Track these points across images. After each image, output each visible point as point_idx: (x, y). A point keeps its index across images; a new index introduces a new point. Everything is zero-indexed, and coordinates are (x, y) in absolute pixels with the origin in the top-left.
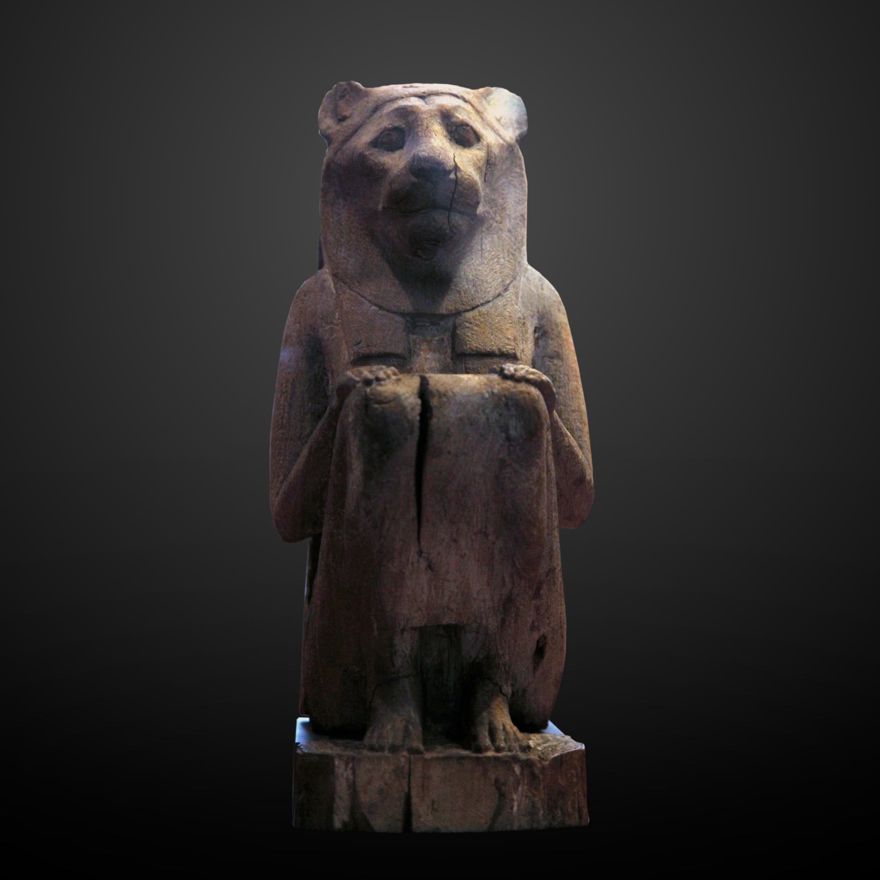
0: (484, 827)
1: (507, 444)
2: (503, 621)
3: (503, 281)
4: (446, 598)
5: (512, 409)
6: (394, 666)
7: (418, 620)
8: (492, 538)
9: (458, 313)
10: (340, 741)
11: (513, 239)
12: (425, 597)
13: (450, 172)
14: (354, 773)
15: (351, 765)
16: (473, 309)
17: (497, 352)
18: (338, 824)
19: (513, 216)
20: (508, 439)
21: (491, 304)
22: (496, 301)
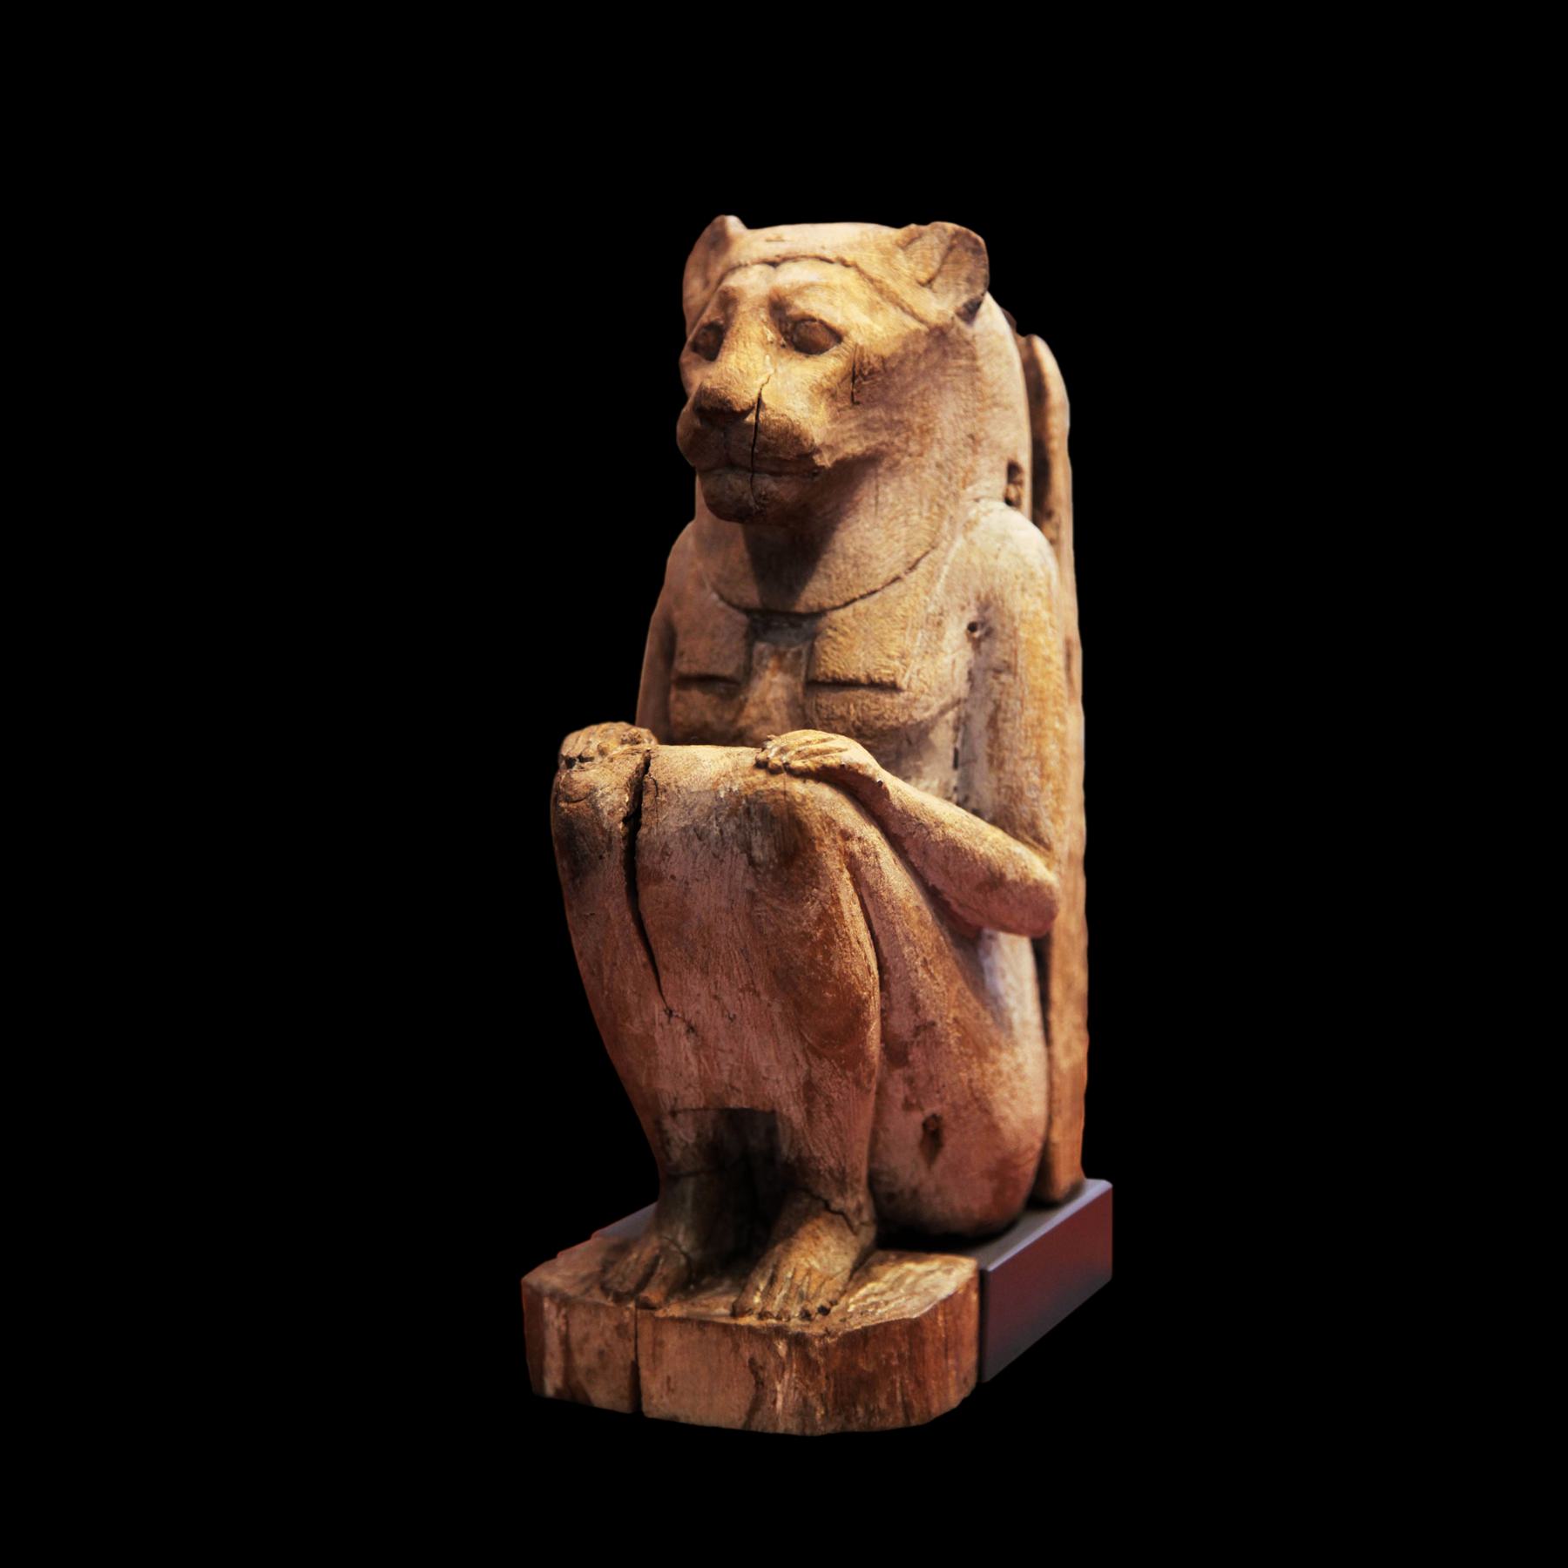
0: (738, 1425)
1: (751, 870)
2: (809, 1113)
3: (908, 555)
4: (726, 1074)
5: (756, 819)
6: (669, 1159)
7: (692, 1098)
8: (765, 998)
9: (821, 612)
11: (945, 480)
12: (694, 1069)
13: (745, 413)
14: (567, 1324)
15: (563, 1311)
16: (847, 604)
17: (863, 679)
18: (550, 1391)
19: (949, 440)
20: (752, 862)
21: (877, 596)
22: (887, 590)
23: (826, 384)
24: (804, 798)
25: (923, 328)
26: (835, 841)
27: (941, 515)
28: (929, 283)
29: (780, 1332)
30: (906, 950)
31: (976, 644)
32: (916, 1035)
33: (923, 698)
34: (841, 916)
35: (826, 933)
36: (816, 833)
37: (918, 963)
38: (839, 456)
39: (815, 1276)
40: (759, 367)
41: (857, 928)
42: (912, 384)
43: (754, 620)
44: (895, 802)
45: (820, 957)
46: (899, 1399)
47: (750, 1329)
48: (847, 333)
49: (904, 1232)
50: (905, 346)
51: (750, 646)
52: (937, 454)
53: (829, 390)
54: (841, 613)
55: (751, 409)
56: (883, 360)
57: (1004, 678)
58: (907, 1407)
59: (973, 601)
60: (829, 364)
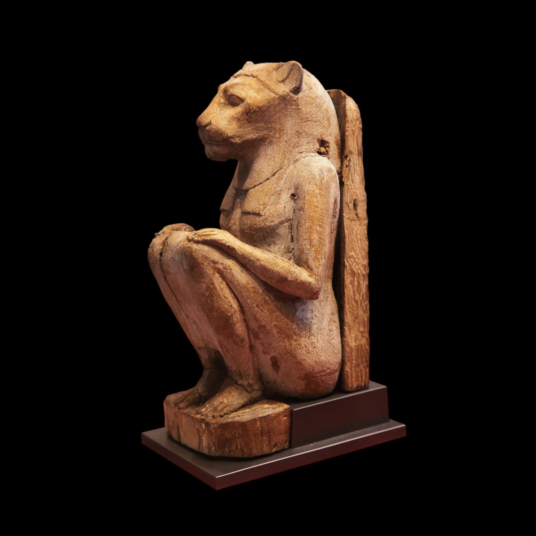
10: (223, 386)
16: (254, 187)
17: (251, 212)
22: (265, 183)
23: (236, 116)
24: (196, 250)
25: (277, 96)
26: (209, 264)
27: (285, 158)
28: (283, 81)
29: (203, 420)
30: (249, 301)
31: (295, 200)
32: (259, 329)
33: (270, 218)
34: (215, 288)
35: (210, 294)
36: (200, 261)
37: (255, 305)
38: (245, 139)
39: (223, 404)
40: (215, 111)
41: (226, 292)
42: (274, 115)
43: (237, 192)
44: (239, 252)
45: (209, 301)
46: (239, 447)
47: (197, 419)
48: (245, 99)
49: (271, 395)
50: (269, 102)
51: (235, 200)
52: (285, 138)
53: (237, 118)
54: (252, 190)
55: (207, 125)
56: (259, 108)
57: (301, 212)
58: (242, 450)
59: (293, 187)
60: (239, 109)
